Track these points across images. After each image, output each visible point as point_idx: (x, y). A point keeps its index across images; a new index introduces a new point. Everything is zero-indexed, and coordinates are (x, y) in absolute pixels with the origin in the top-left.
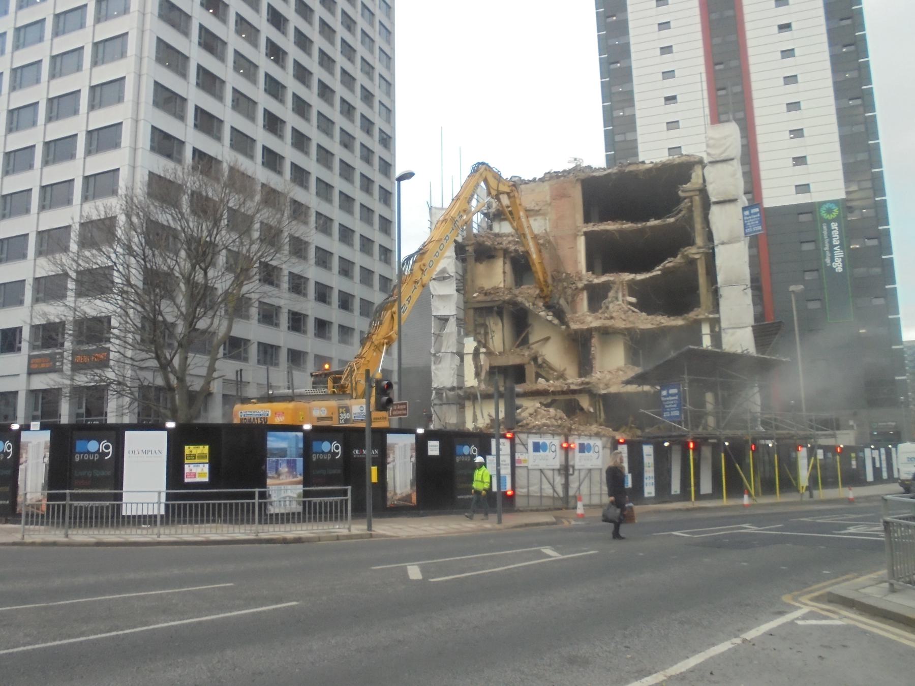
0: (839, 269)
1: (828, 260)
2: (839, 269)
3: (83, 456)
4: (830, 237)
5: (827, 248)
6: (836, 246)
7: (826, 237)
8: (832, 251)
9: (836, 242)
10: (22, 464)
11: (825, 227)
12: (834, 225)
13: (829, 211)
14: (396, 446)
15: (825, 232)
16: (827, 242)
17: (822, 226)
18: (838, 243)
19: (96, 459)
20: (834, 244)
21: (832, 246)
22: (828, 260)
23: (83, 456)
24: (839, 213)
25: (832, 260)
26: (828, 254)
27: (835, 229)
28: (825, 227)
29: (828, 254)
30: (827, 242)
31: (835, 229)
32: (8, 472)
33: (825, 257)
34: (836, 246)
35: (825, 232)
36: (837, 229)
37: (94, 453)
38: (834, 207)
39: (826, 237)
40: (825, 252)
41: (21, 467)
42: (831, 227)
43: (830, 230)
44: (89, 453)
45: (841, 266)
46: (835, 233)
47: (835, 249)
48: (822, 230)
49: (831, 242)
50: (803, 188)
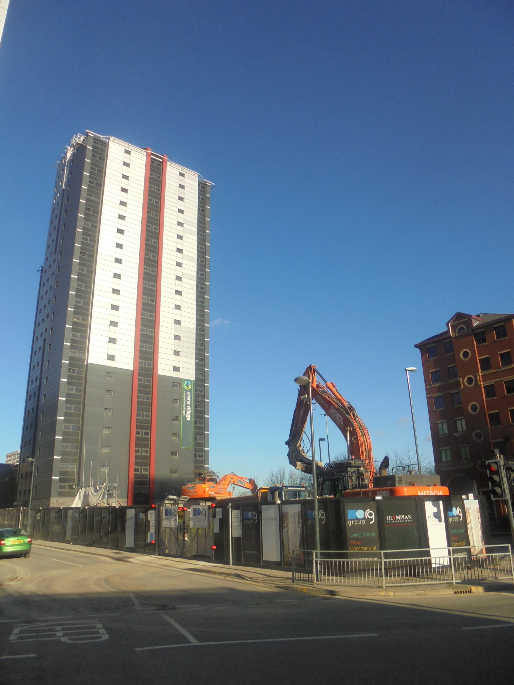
0: (189, 419)
1: (184, 412)
2: (189, 419)
3: (354, 522)
4: (187, 400)
5: (184, 405)
6: (189, 405)
7: (184, 399)
8: (186, 408)
9: (189, 403)
10: (469, 524)
11: (185, 393)
12: (189, 394)
13: (187, 385)
14: (288, 514)
15: (184, 396)
16: (185, 401)
17: (183, 393)
18: (189, 404)
19: (363, 523)
20: (188, 404)
21: (187, 405)
22: (184, 412)
23: (354, 522)
24: (192, 387)
25: (186, 413)
26: (185, 409)
27: (189, 396)
28: (185, 393)
29: (185, 409)
30: (185, 401)
31: (189, 396)
32: (462, 531)
33: (183, 411)
34: (189, 405)
35: (184, 396)
36: (190, 395)
37: (362, 519)
38: (189, 384)
39: (184, 399)
40: (183, 407)
41: (469, 526)
42: (187, 394)
43: (187, 396)
44: (357, 519)
45: (189, 417)
46: (189, 398)
47: (188, 407)
48: (183, 395)
49: (186, 402)
50: (176, 369)
